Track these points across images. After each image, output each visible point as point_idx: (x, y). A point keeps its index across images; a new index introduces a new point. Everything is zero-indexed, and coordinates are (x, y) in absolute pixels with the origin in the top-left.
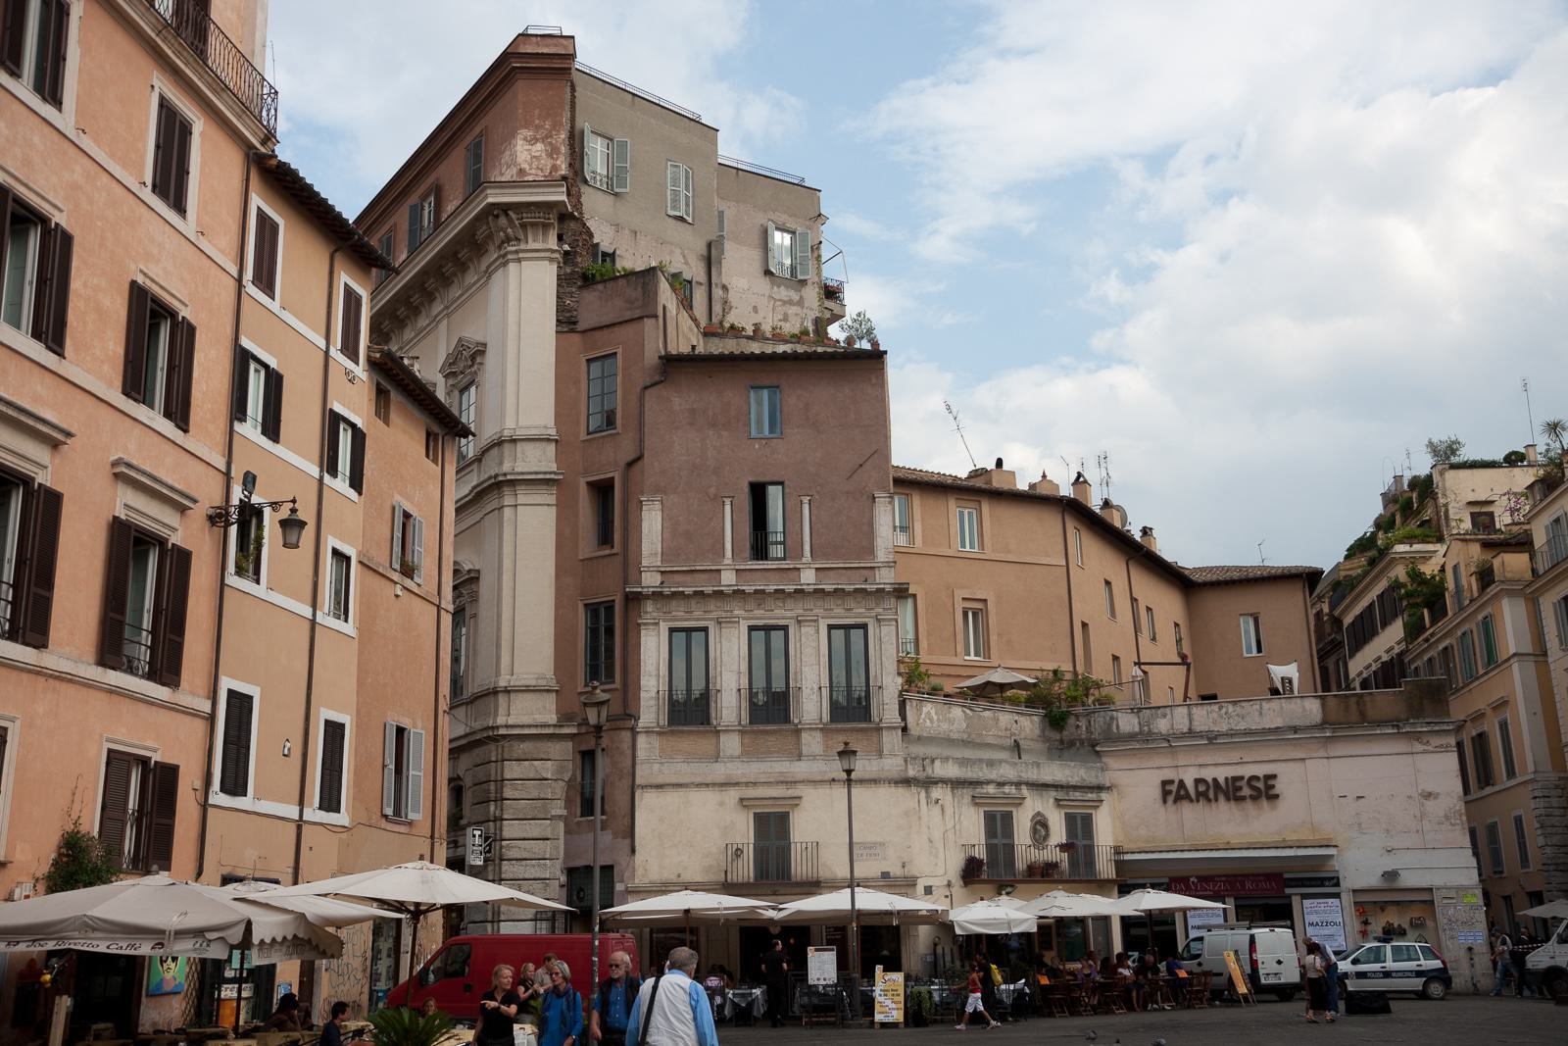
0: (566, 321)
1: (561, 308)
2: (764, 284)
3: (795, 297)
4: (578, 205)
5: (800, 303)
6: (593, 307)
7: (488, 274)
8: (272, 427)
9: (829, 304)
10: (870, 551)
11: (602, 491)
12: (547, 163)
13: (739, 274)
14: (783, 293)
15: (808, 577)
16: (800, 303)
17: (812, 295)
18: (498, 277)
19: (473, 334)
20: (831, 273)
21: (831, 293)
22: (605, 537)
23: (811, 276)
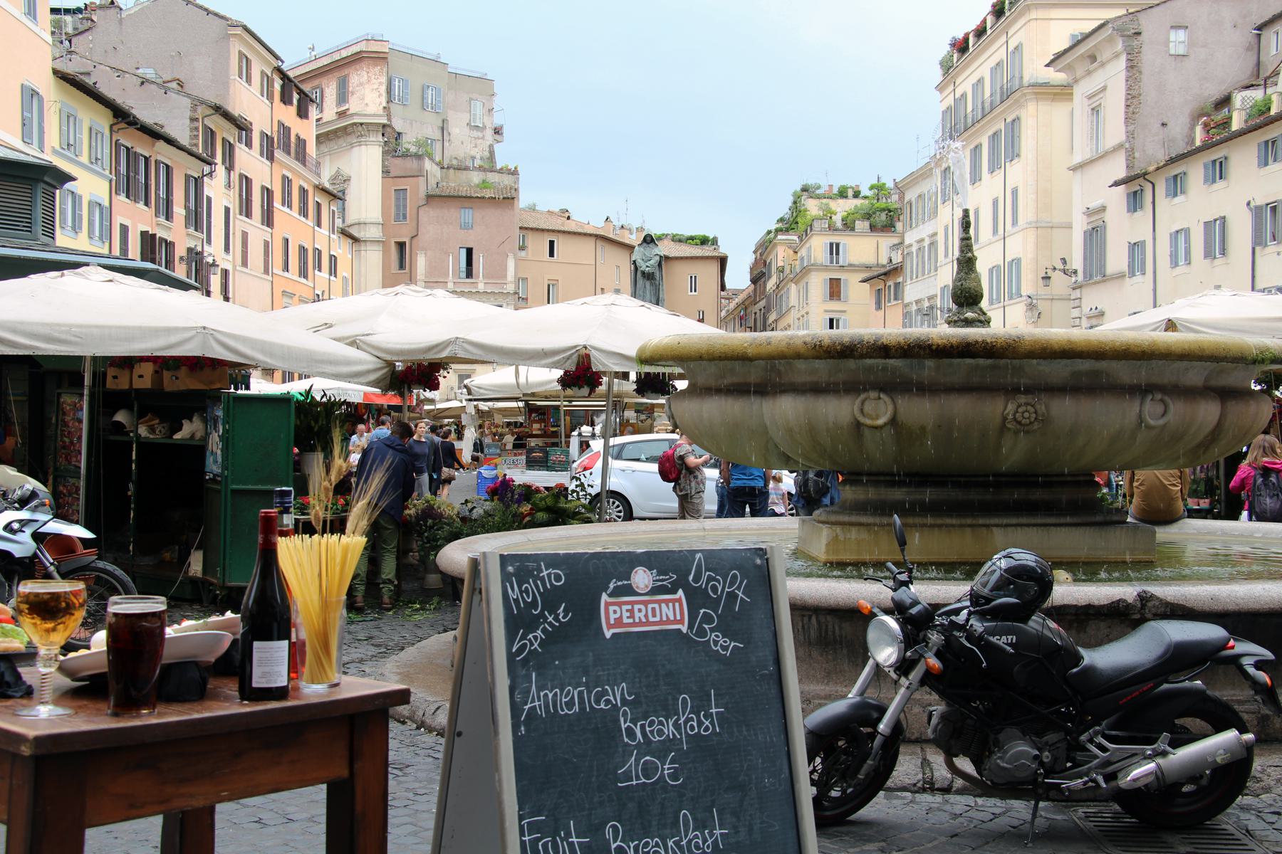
0: (386, 172)
1: (383, 166)
2: (467, 129)
3: (480, 135)
4: (389, 119)
5: (483, 138)
6: (398, 165)
7: (352, 146)
8: (320, 270)
9: (497, 137)
10: (505, 276)
11: (401, 246)
12: (378, 101)
13: (458, 130)
14: (476, 134)
15: (481, 287)
16: (483, 138)
17: (489, 133)
18: (356, 149)
19: (346, 171)
20: (497, 120)
21: (498, 131)
22: (402, 266)
23: (488, 125)
